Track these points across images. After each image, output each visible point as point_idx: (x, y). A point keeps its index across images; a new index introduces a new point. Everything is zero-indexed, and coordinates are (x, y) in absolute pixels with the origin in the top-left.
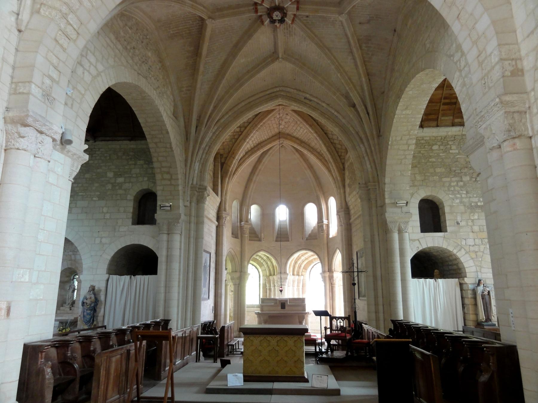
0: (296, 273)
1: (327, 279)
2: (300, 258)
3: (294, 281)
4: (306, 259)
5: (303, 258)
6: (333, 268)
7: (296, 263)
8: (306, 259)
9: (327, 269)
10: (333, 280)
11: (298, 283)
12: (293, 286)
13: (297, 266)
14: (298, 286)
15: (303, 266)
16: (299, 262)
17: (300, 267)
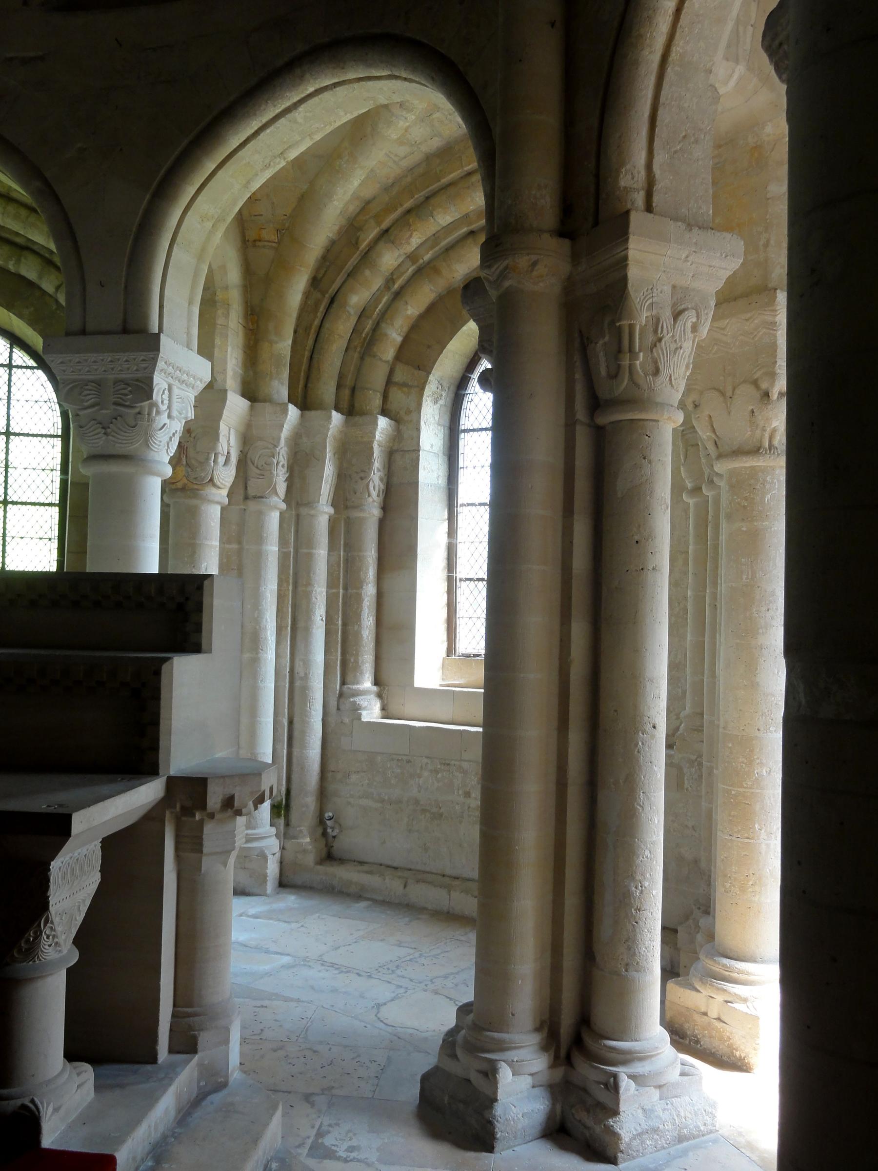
0: (327, 389)
1: (542, 335)
2: (367, 258)
3: (301, 464)
4: (424, 271)
5: (389, 259)
6: (631, 176)
7: (325, 295)
8: (424, 271)
9: (540, 190)
10: (620, 346)
11: (342, 477)
12: (298, 496)
13: (342, 328)
14: (345, 498)
15: (394, 335)
16: (357, 299)
17: (365, 343)
